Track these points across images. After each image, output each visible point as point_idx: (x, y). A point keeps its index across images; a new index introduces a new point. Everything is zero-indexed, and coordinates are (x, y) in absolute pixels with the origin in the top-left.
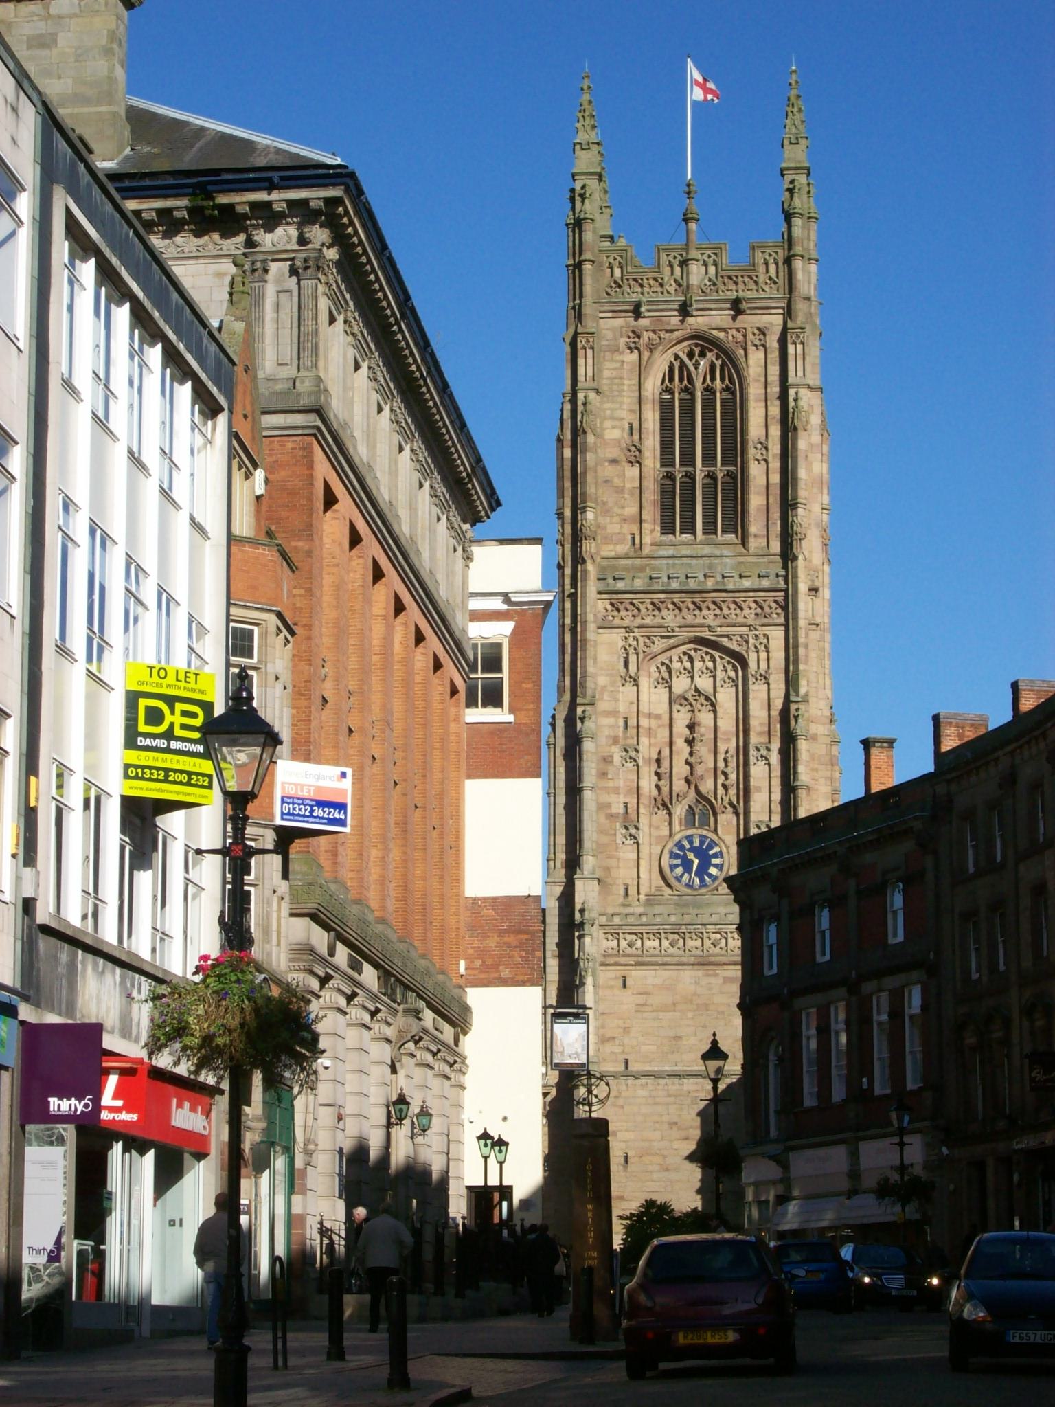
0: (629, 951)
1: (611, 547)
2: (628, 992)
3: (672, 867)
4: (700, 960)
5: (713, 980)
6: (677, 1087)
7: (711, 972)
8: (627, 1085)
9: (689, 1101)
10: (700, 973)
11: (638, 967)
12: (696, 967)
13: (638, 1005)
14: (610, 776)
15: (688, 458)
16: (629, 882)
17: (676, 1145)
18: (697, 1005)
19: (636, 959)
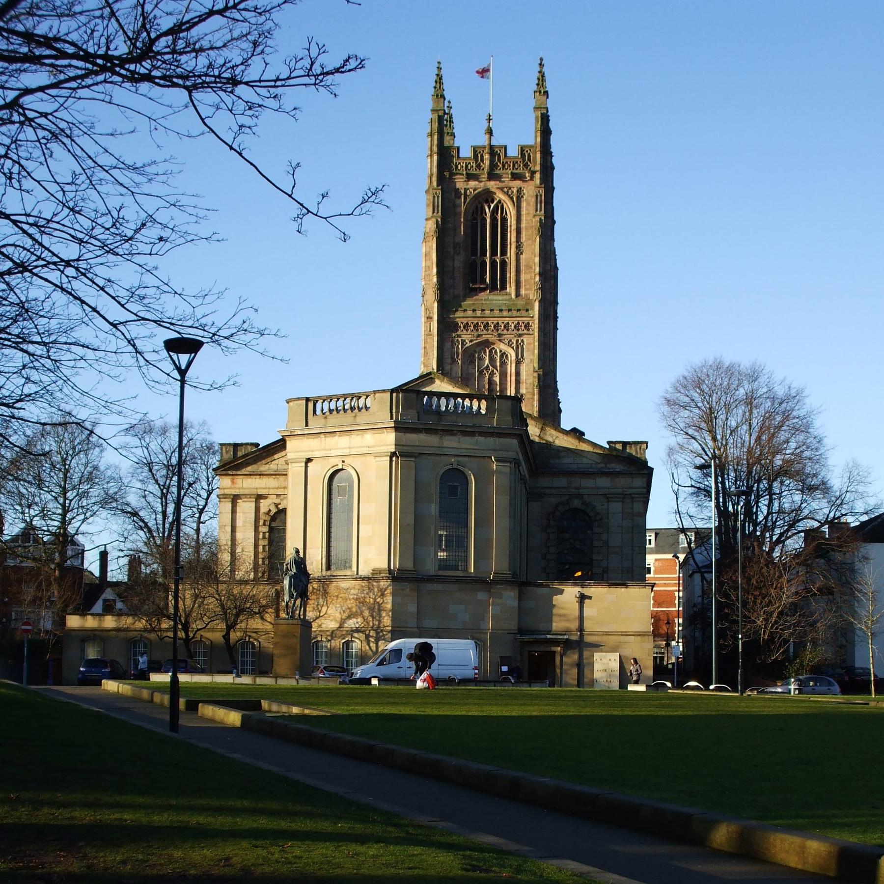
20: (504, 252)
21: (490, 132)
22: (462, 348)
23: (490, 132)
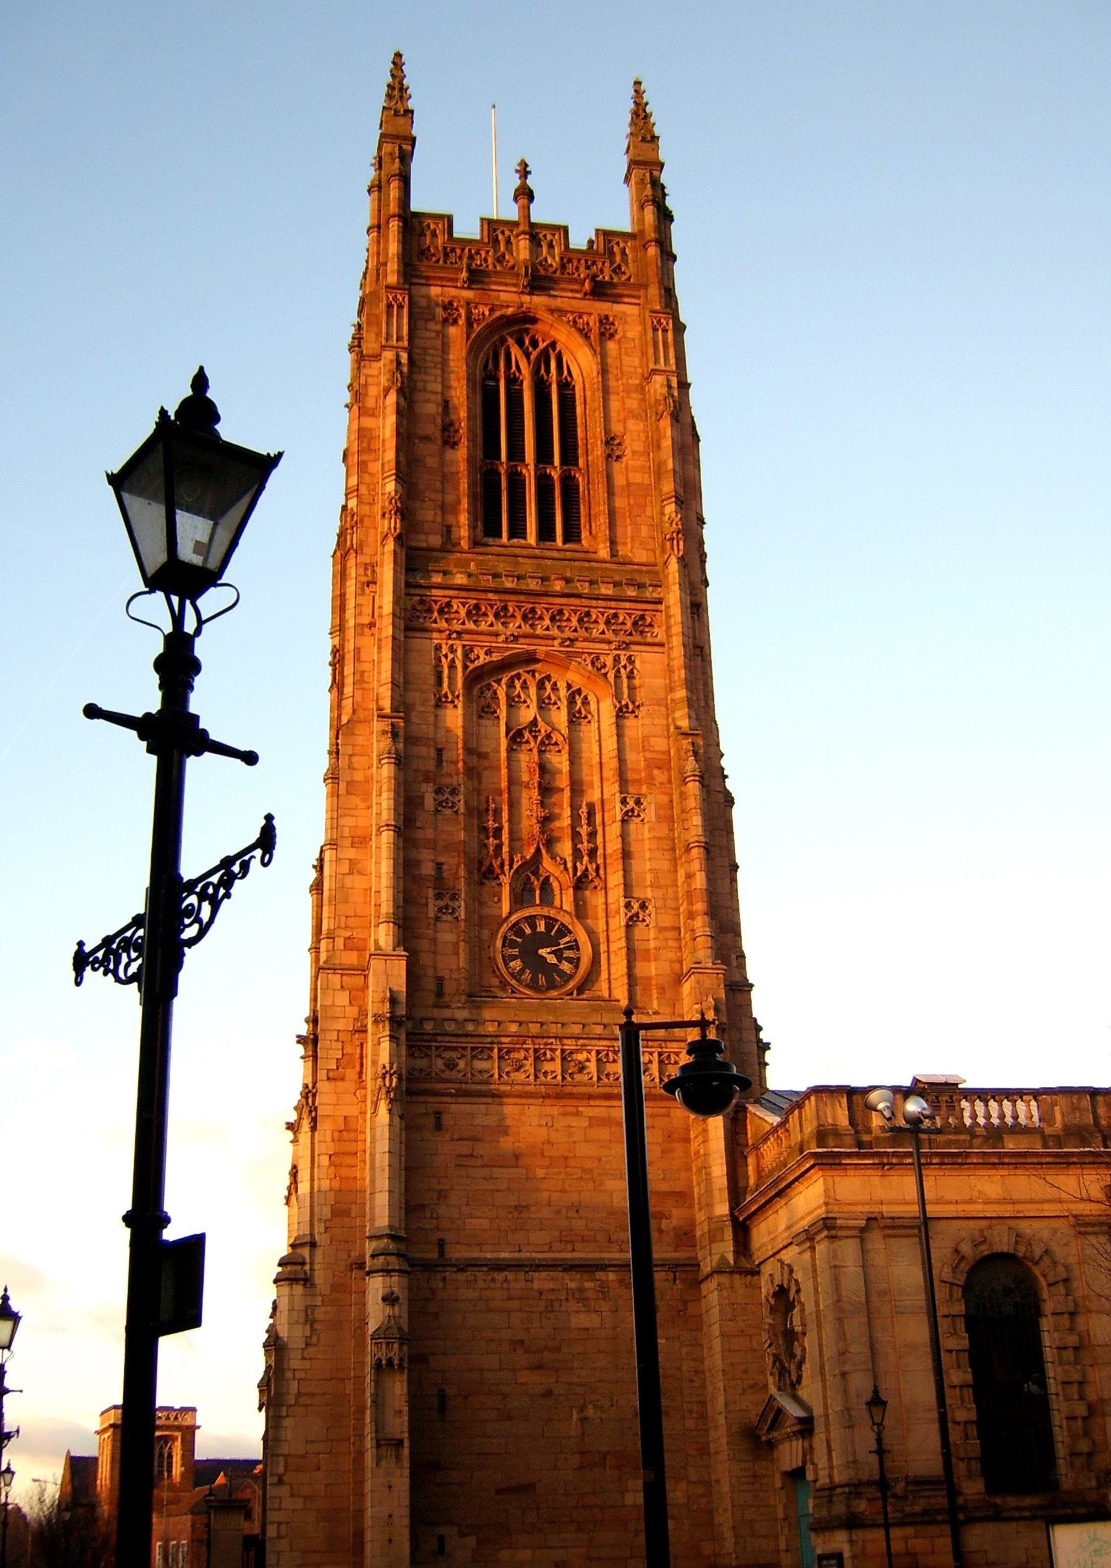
0: (447, 1074)
1: (423, 537)
2: (447, 1137)
3: (507, 960)
4: (551, 1091)
5: (573, 1121)
6: (522, 1285)
7: (570, 1109)
8: (444, 1279)
9: (542, 1304)
10: (555, 1111)
11: (460, 1100)
12: (548, 1102)
13: (459, 1156)
14: (418, 824)
15: (516, 451)
16: (445, 974)
17: (525, 1377)
18: (550, 1157)
19: (457, 1086)
20: (570, 455)
21: (525, 195)
22: (465, 667)
23: (525, 195)
